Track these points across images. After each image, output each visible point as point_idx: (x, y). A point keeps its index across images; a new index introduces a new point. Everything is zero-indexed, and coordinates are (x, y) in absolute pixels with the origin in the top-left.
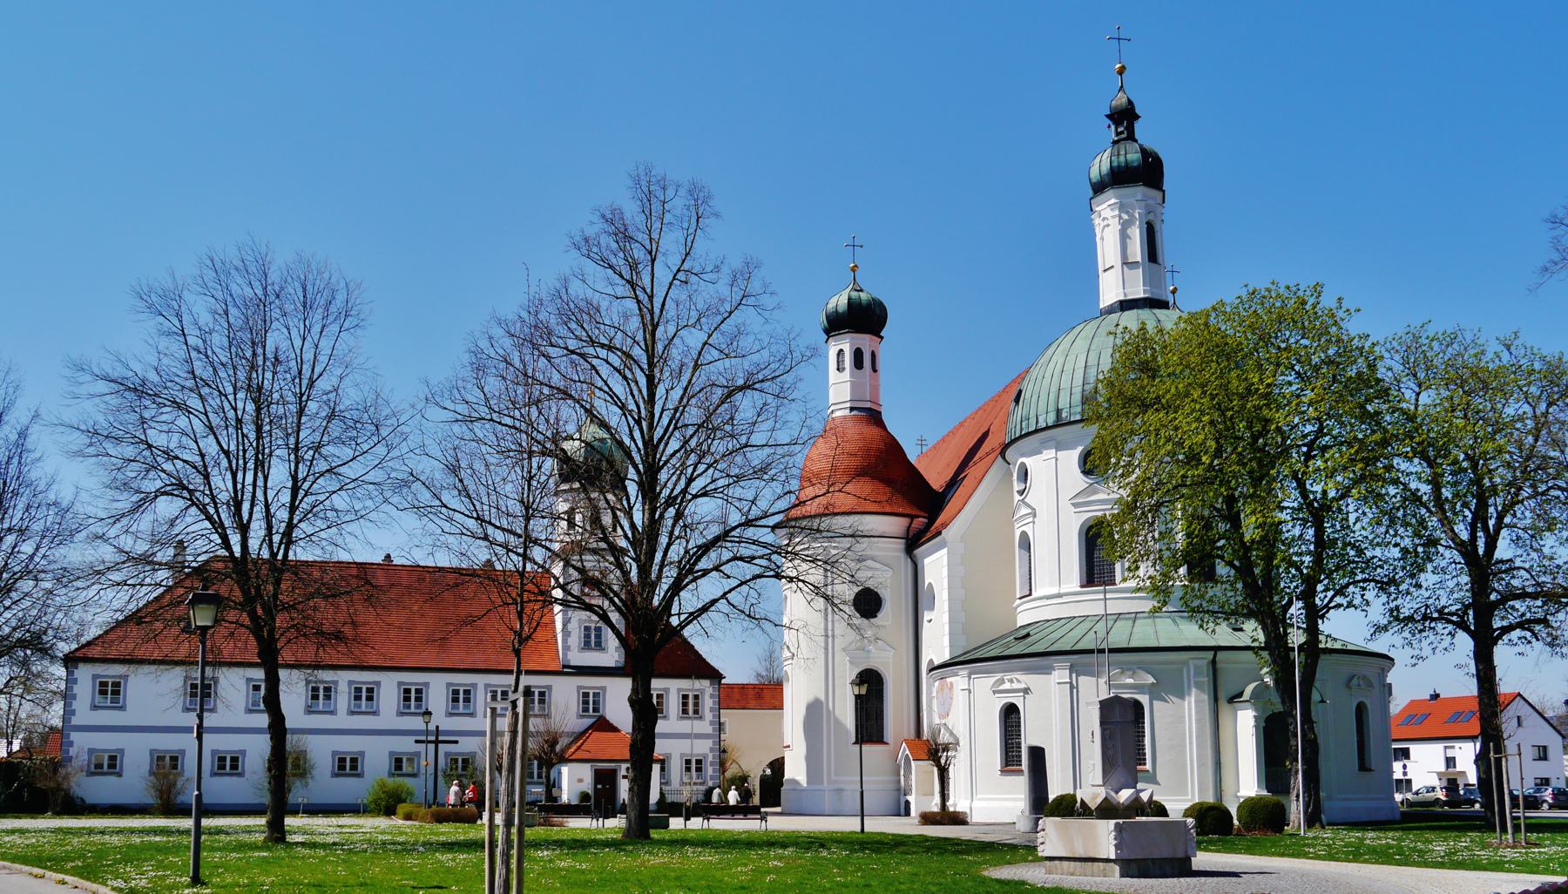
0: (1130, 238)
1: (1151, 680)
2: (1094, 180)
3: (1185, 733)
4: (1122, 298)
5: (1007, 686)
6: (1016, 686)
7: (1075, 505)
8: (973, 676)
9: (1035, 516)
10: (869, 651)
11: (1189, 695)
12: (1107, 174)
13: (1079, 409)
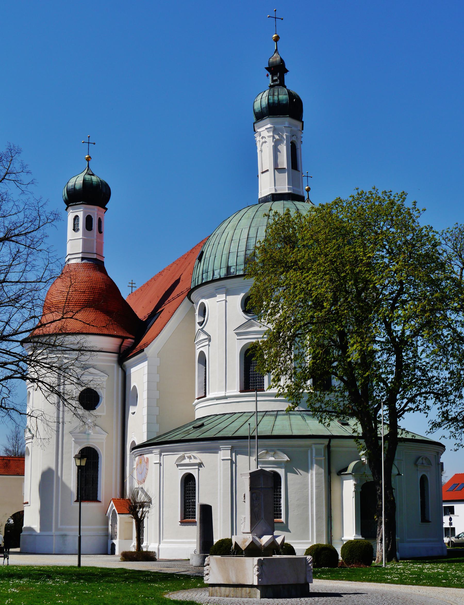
0: (280, 152)
1: (286, 458)
2: (257, 111)
3: (308, 496)
4: (273, 192)
5: (187, 461)
6: (193, 461)
7: (238, 334)
8: (163, 454)
9: (210, 340)
10: (89, 434)
11: (312, 469)
12: (266, 108)
13: (242, 267)
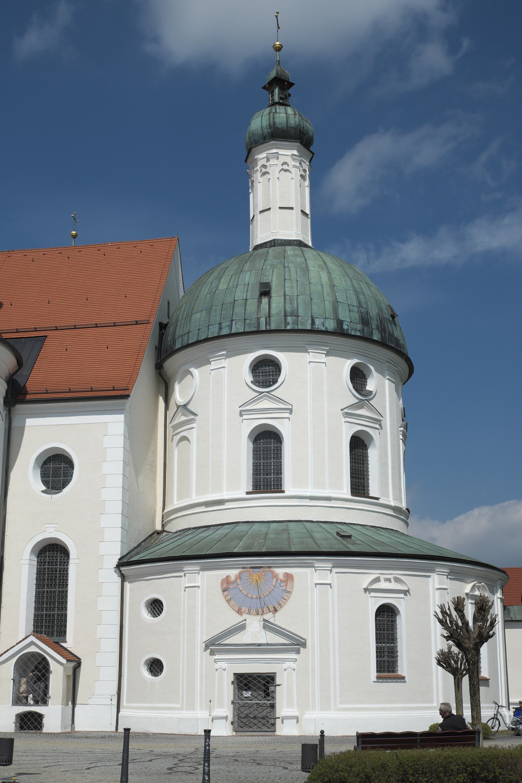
2: (278, 125)
5: (383, 585)
8: (335, 570)
9: (291, 411)
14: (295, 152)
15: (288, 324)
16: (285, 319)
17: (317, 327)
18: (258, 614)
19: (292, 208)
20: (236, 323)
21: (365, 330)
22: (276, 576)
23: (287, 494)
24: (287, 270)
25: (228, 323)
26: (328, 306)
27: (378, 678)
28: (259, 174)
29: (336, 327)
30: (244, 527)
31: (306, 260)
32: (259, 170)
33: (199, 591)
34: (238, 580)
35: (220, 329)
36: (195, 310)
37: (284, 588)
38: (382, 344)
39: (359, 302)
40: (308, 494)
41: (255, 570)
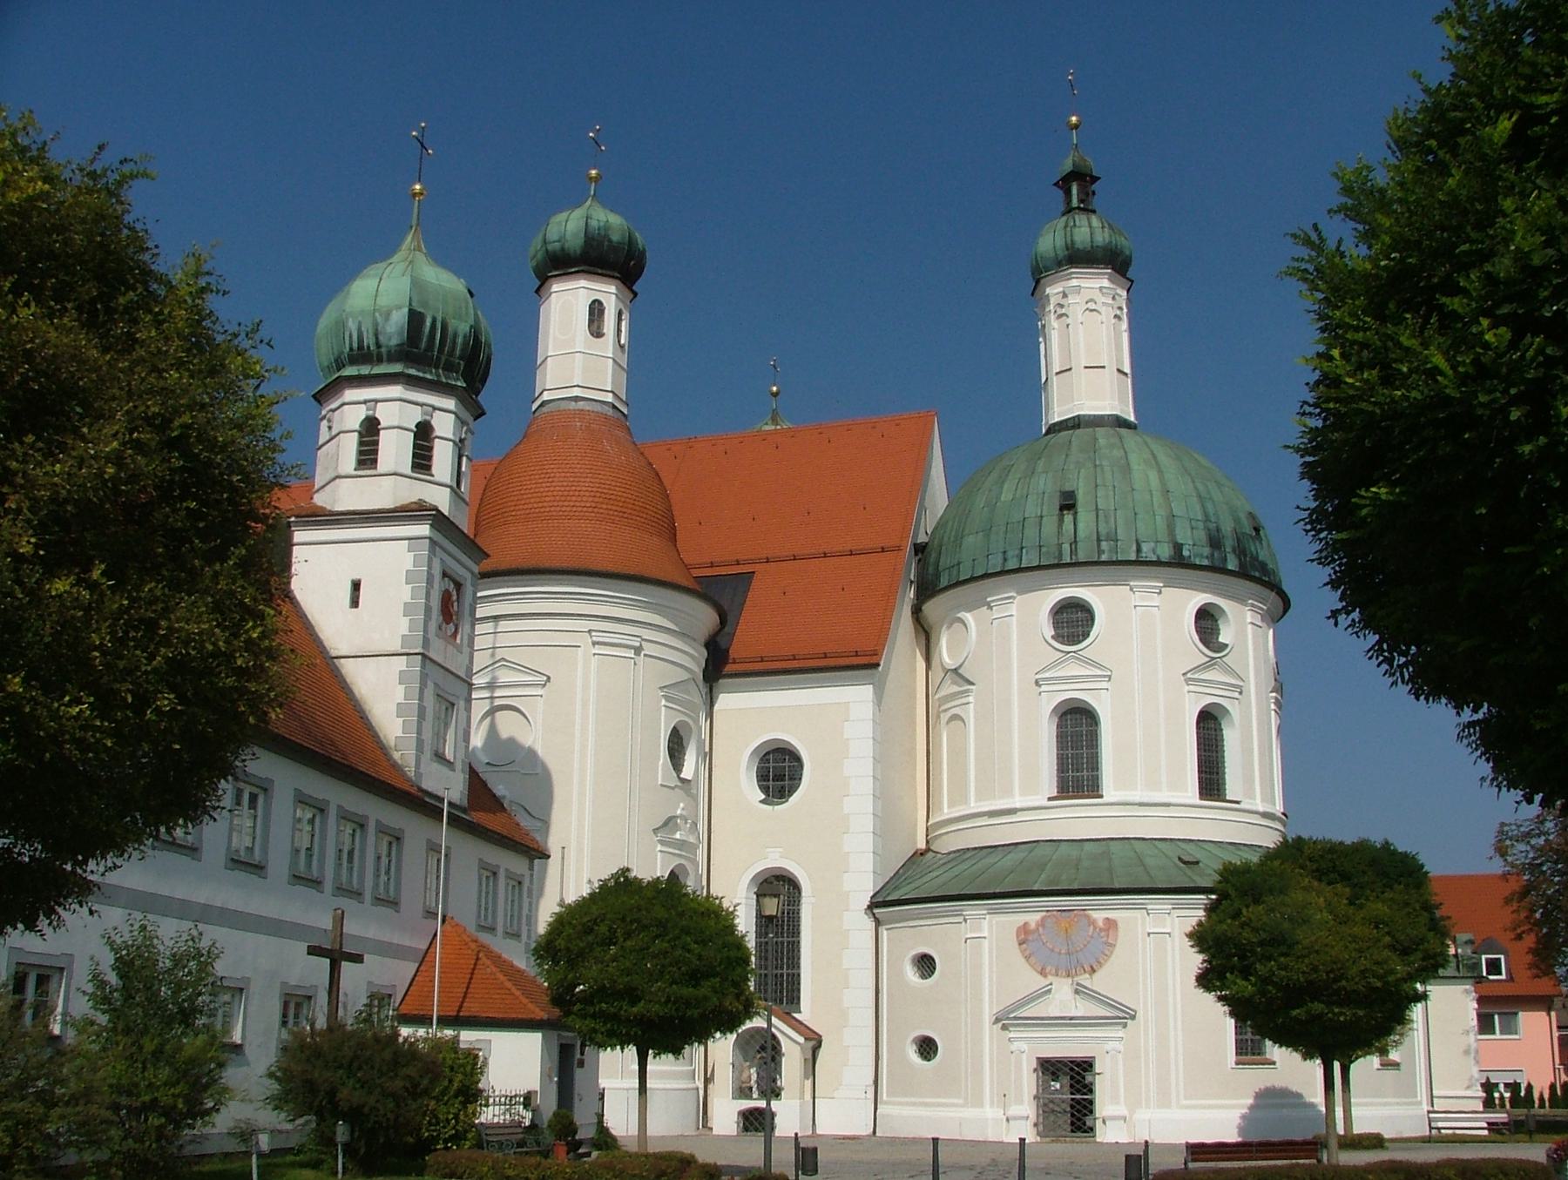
2: (1079, 245)
14: (1106, 283)
15: (1104, 552)
16: (1099, 546)
17: (1144, 555)
18: (1068, 976)
19: (1104, 367)
20: (1027, 553)
21: (1216, 555)
22: (1093, 923)
23: (1106, 799)
24: (1098, 469)
25: (1017, 552)
26: (1161, 522)
27: (1237, 1064)
28: (1053, 317)
29: (1173, 553)
30: (1048, 849)
31: (1126, 452)
32: (1053, 311)
33: (987, 940)
34: (1041, 929)
35: (1005, 560)
36: (967, 532)
37: (1104, 939)
38: (1243, 574)
39: (1206, 515)
40: (1137, 799)
41: (1064, 914)
